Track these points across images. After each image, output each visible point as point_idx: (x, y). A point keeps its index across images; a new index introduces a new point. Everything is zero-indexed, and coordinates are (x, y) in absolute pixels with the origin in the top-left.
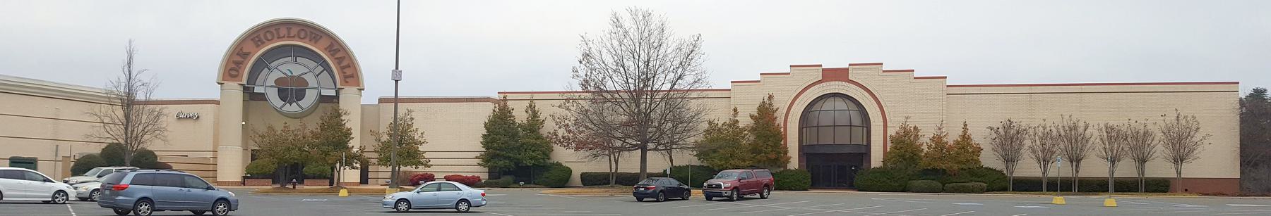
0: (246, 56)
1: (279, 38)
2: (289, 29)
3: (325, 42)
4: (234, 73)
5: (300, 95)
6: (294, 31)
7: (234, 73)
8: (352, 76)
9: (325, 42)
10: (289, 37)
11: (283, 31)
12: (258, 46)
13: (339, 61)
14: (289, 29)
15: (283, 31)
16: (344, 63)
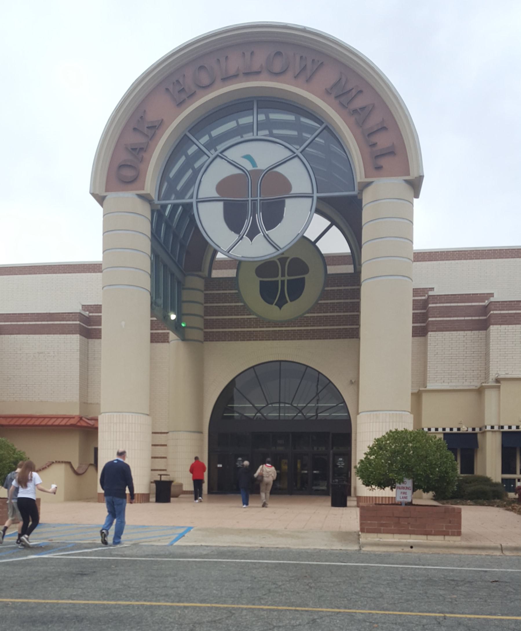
0: (155, 128)
12: (180, 104)
13: (359, 116)
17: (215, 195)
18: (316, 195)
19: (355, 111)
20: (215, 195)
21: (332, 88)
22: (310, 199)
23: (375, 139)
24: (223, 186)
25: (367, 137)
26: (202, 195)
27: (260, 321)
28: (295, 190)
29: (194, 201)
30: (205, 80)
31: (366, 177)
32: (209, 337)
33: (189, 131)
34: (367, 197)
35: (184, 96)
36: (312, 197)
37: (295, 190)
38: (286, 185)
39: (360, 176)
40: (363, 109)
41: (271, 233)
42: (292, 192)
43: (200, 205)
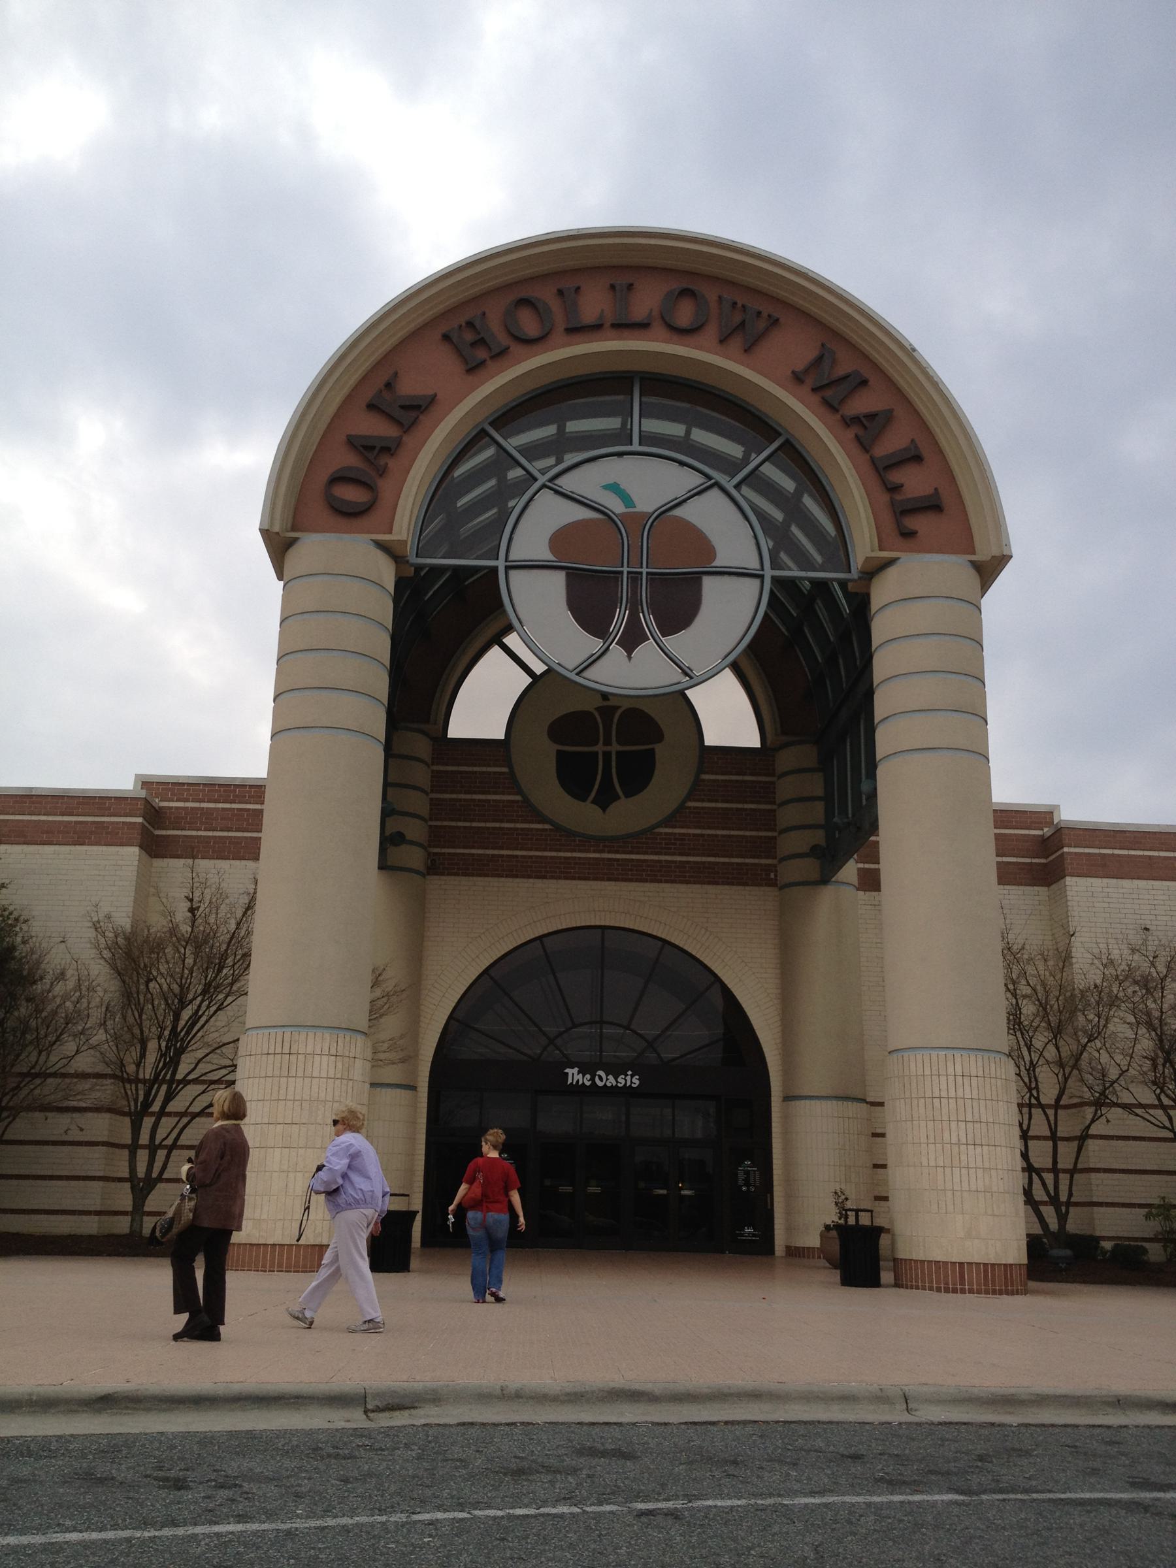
0: (413, 412)
1: (576, 330)
2: (622, 292)
3: (793, 347)
4: (351, 494)
5: (637, 773)
6: (647, 299)
7: (351, 494)
8: (932, 505)
9: (793, 347)
10: (624, 326)
11: (594, 302)
12: (474, 368)
13: (865, 430)
14: (622, 292)
15: (594, 302)
16: (892, 442)
17: (546, 555)
18: (769, 573)
19: (856, 420)
20: (544, 554)
21: (806, 371)
22: (757, 582)
23: (896, 477)
24: (559, 540)
25: (883, 472)
26: (517, 554)
27: (565, 836)
28: (722, 559)
29: (501, 564)
30: (529, 324)
31: (880, 550)
32: (435, 867)
33: (491, 424)
34: (882, 592)
35: (481, 354)
36: (761, 577)
37: (722, 559)
38: (705, 549)
39: (864, 543)
40: (872, 416)
41: (669, 642)
42: (718, 562)
43: (513, 574)
